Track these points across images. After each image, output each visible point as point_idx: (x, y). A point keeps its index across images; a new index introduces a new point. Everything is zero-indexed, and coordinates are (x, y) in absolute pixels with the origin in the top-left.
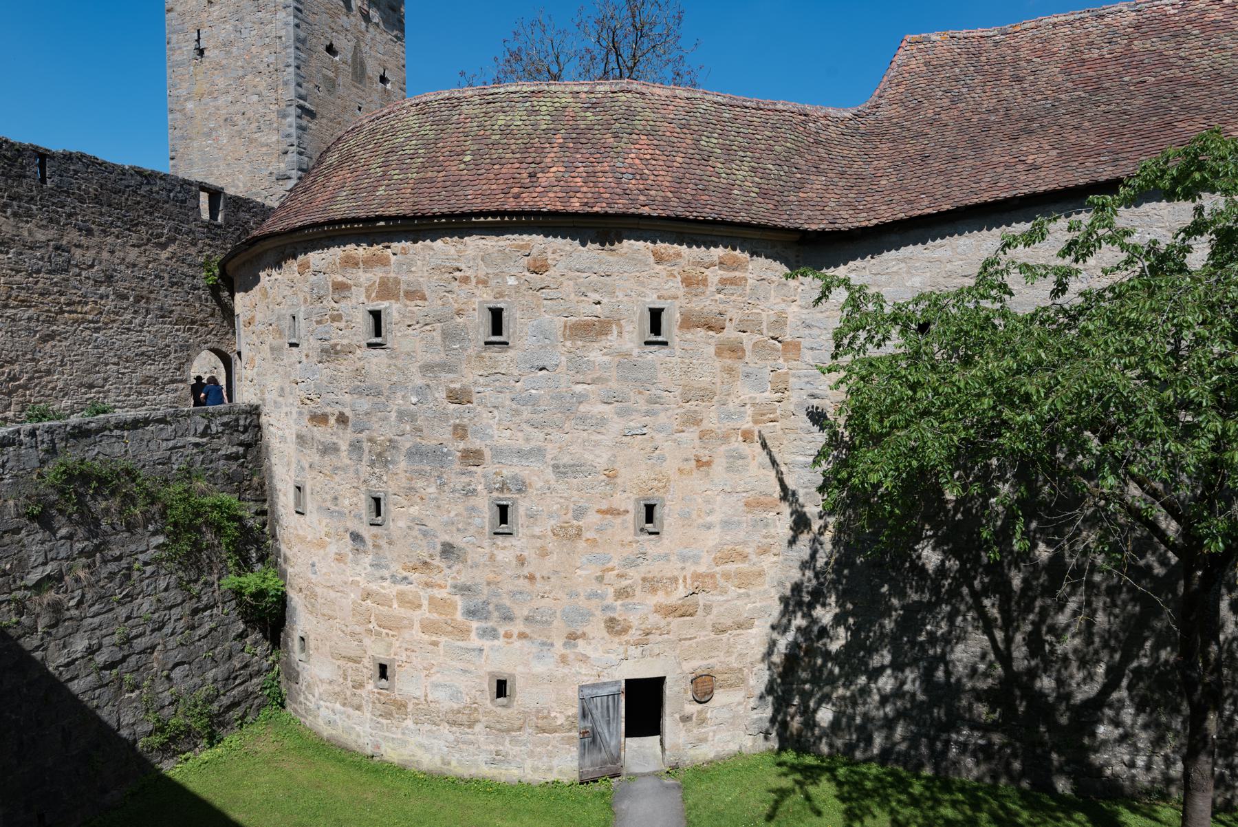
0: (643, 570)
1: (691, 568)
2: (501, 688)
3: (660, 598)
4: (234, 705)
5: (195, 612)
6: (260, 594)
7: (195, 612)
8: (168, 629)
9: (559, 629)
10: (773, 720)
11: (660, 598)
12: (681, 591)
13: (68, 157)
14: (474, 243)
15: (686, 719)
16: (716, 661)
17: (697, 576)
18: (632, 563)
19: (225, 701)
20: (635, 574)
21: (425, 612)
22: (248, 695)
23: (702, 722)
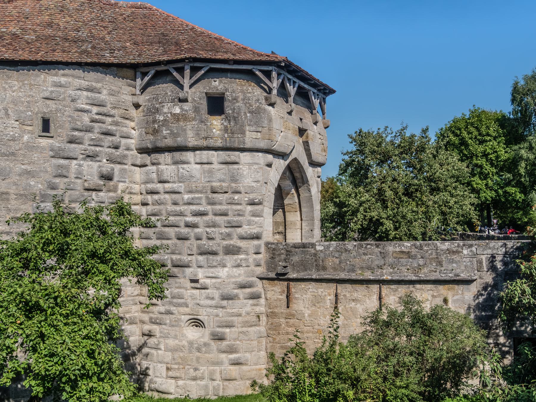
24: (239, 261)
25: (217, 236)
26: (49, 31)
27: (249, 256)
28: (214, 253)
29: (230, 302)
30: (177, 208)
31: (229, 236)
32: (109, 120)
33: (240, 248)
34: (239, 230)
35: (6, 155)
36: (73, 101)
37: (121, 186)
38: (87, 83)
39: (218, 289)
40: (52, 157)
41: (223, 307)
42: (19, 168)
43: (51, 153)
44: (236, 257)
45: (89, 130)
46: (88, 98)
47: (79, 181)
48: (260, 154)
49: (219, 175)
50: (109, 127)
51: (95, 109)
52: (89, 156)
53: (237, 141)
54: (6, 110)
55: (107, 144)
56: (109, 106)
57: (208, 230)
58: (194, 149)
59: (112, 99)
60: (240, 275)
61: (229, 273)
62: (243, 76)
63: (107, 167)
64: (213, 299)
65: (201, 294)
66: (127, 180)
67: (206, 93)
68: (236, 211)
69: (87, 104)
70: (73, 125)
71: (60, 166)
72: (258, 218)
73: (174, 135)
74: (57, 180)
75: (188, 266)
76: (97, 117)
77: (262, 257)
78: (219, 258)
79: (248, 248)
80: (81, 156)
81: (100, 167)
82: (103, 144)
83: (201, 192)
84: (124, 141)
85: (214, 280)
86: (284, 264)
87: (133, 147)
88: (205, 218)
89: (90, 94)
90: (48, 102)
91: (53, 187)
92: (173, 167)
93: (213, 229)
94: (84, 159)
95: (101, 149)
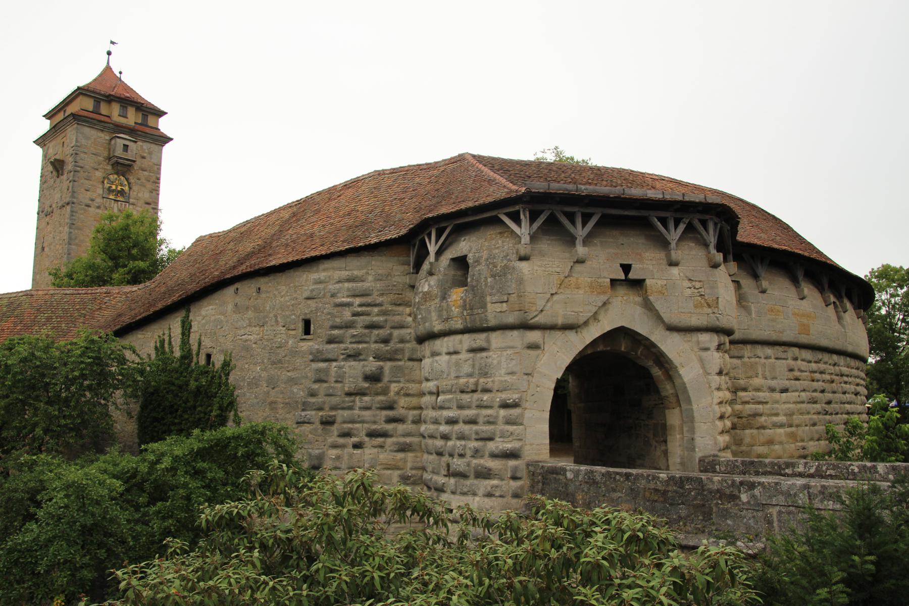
24: (489, 488)
27: (504, 482)
28: (463, 476)
31: (476, 453)
32: (376, 310)
33: (490, 470)
34: (491, 446)
35: (275, 363)
37: (394, 387)
38: (347, 273)
40: (312, 361)
42: (285, 375)
43: (311, 357)
44: (487, 482)
46: (348, 290)
47: (339, 385)
48: (515, 333)
49: (466, 369)
50: (375, 319)
51: (358, 301)
52: (349, 356)
53: (478, 319)
54: (276, 316)
55: (373, 339)
56: (376, 293)
63: (372, 365)
66: (402, 379)
67: (453, 260)
68: (485, 417)
69: (348, 296)
70: (331, 323)
71: (319, 370)
72: (515, 427)
74: (316, 386)
76: (359, 309)
78: (468, 482)
79: (500, 470)
80: (342, 357)
81: (364, 366)
82: (368, 339)
84: (396, 333)
90: (309, 302)
91: (313, 394)
93: (463, 443)
94: (345, 360)
95: (365, 345)
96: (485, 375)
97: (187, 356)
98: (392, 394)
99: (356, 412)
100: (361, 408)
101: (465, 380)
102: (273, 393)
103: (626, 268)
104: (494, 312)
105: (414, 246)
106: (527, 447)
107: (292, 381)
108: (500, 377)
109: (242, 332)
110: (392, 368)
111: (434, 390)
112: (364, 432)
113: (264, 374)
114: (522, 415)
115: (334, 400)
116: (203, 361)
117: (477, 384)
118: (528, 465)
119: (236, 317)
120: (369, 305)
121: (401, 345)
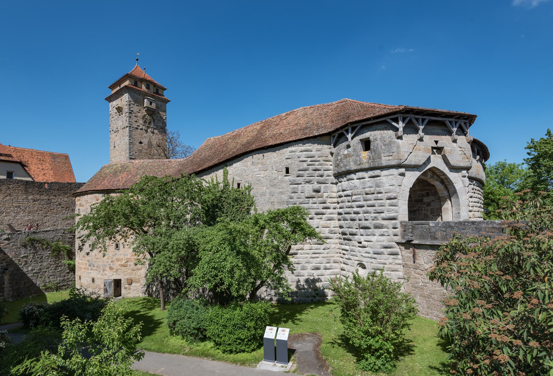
0: (116, 257)
1: (126, 257)
2: (93, 280)
3: (120, 263)
4: (63, 286)
5: (57, 267)
6: (69, 264)
7: (57, 267)
8: (50, 269)
9: (102, 268)
10: (146, 290)
11: (120, 263)
12: (124, 262)
13: (52, 183)
14: (90, 196)
15: (126, 288)
16: (133, 276)
17: (127, 259)
18: (114, 255)
19: (61, 284)
20: (115, 258)
21: (84, 266)
22: (68, 285)
23: (130, 289)
25: (370, 218)
26: (295, 128)
28: (368, 228)
29: (379, 255)
30: (350, 204)
31: (375, 218)
32: (317, 163)
36: (298, 157)
39: (372, 248)
41: (375, 258)
44: (381, 230)
45: (305, 170)
46: (305, 155)
47: (303, 194)
49: (369, 184)
50: (317, 167)
51: (309, 159)
54: (272, 167)
55: (316, 175)
56: (317, 156)
57: (365, 215)
58: (355, 172)
59: (318, 152)
60: (385, 240)
61: (377, 240)
62: (379, 126)
63: (316, 186)
64: (369, 253)
65: (363, 250)
70: (298, 169)
71: (294, 188)
73: (345, 166)
74: (293, 195)
75: (356, 235)
77: (399, 231)
83: (359, 194)
84: (326, 172)
85: (369, 243)
86: (412, 235)
87: (331, 174)
88: (363, 209)
89: (306, 153)
92: (347, 182)
93: (367, 214)
94: (305, 184)
96: (379, 186)
97: (226, 185)
98: (325, 197)
99: (310, 205)
100: (312, 203)
101: (369, 189)
102: (272, 198)
103: (436, 142)
104: (385, 161)
105: (334, 137)
106: (400, 215)
107: (282, 193)
108: (386, 187)
109: (256, 173)
110: (325, 187)
111: (350, 194)
112: (314, 213)
113: (268, 191)
114: (398, 202)
115: (301, 200)
116: (236, 186)
117: (374, 190)
118: (401, 223)
119: (252, 167)
120: (314, 161)
121: (328, 177)
